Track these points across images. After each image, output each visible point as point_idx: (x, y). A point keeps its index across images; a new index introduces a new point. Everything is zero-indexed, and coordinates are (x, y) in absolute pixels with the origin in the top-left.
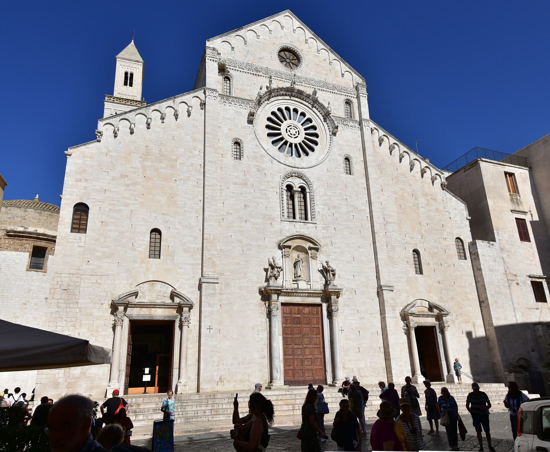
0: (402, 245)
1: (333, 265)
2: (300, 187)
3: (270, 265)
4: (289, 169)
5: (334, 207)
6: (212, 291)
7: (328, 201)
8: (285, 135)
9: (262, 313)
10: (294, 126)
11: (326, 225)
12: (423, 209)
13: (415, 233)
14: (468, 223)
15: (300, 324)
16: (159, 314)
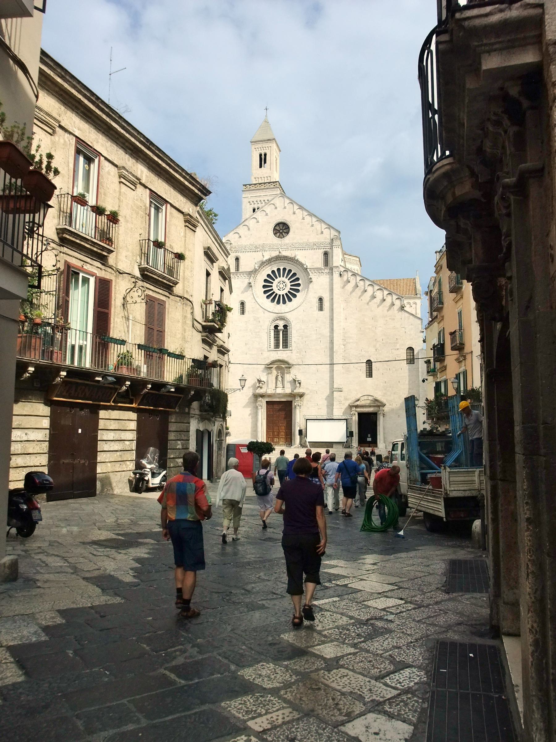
1: (299, 378)
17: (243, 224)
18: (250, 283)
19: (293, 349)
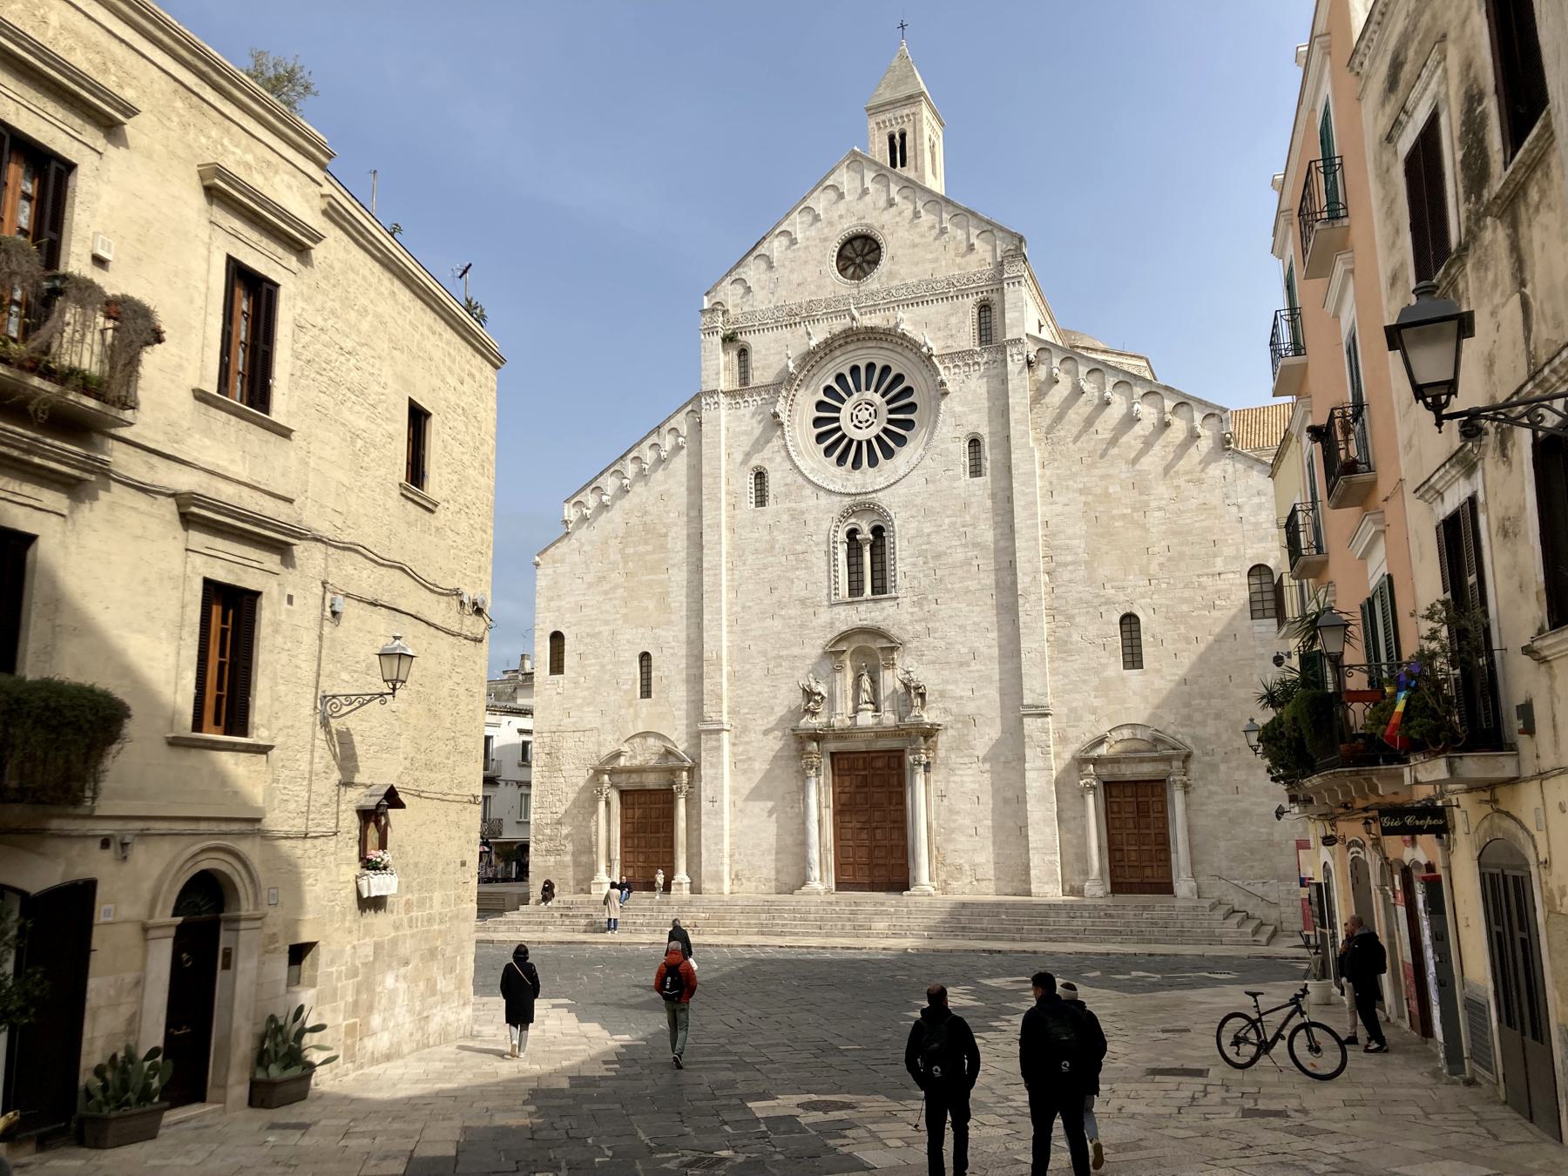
0: (1091, 610)
3: (804, 690)
4: (847, 501)
5: (938, 556)
9: (798, 772)
12: (1161, 513)
13: (1131, 577)
16: (652, 781)
17: (756, 253)
18: (776, 415)
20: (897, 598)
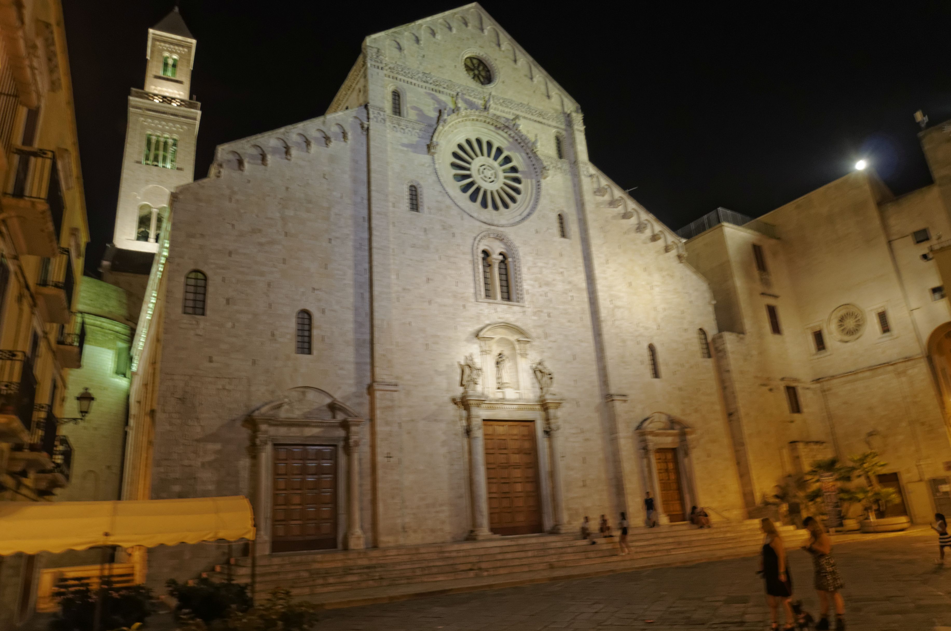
2: (501, 254)
5: (547, 284)
6: (389, 403)
7: (540, 276)
8: (477, 177)
10: (489, 166)
11: (539, 309)
14: (711, 309)
15: (505, 449)
19: (526, 304)
20: (523, 307)
